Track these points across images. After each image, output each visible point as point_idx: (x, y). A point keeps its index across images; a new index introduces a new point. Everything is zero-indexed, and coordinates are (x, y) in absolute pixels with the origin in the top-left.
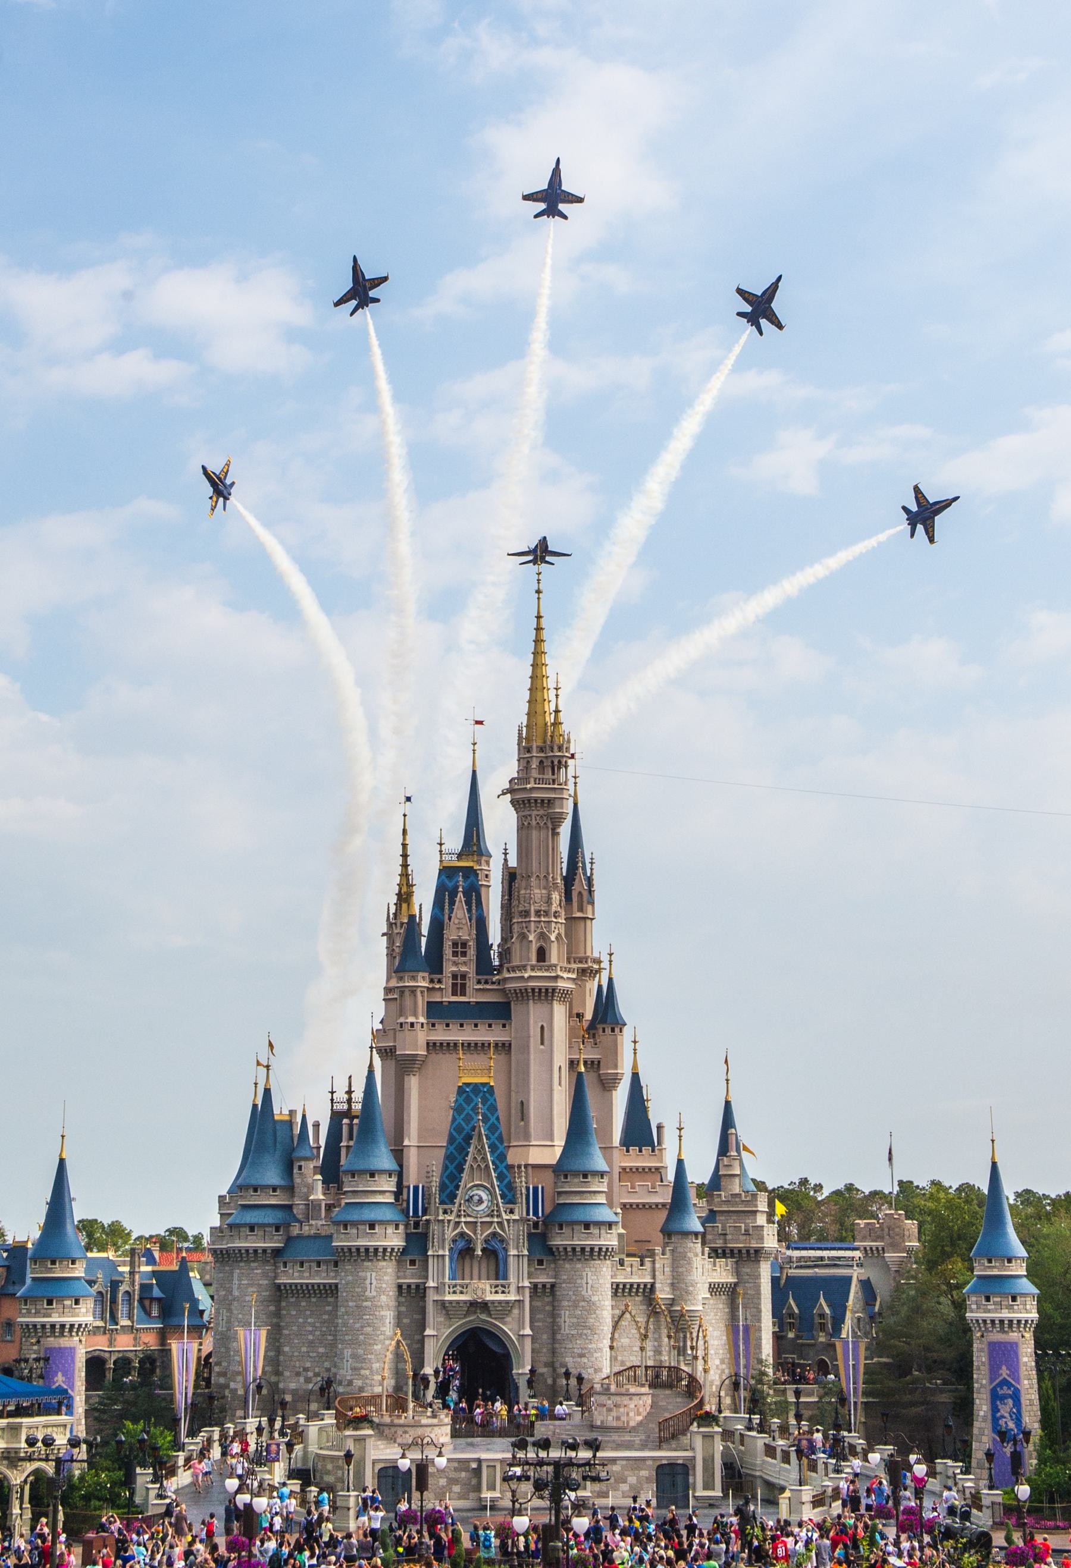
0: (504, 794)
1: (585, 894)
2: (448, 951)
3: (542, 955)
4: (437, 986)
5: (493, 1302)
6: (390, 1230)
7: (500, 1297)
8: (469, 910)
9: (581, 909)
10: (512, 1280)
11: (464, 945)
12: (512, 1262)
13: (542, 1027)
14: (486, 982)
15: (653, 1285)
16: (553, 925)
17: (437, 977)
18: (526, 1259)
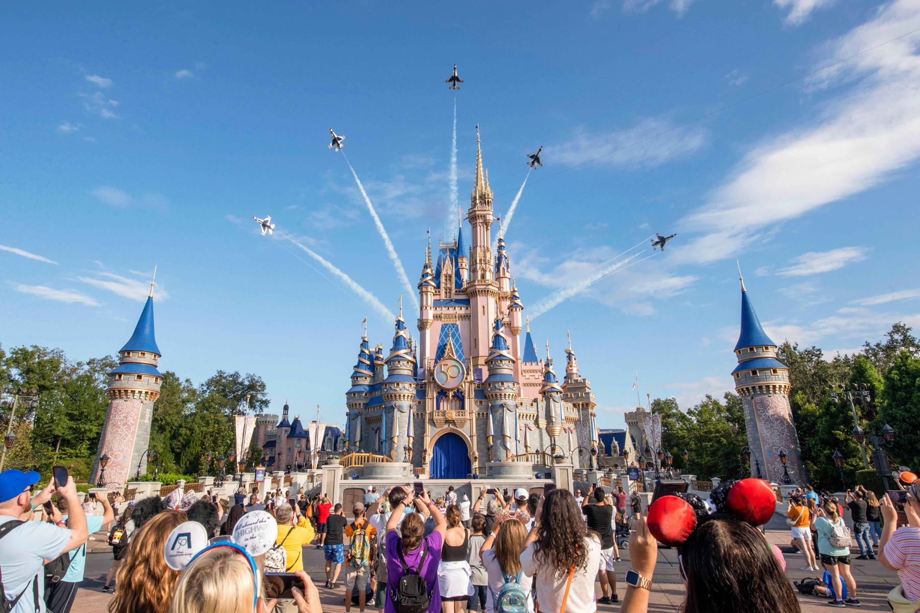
0: (467, 219)
1: (506, 268)
2: (443, 279)
3: (483, 276)
4: (438, 293)
5: (457, 419)
6: (407, 386)
7: (461, 417)
8: (452, 263)
9: (504, 274)
10: (466, 409)
11: (450, 277)
12: (467, 401)
13: (484, 307)
14: (459, 292)
15: (538, 416)
16: (487, 265)
17: (437, 291)
18: (473, 400)
